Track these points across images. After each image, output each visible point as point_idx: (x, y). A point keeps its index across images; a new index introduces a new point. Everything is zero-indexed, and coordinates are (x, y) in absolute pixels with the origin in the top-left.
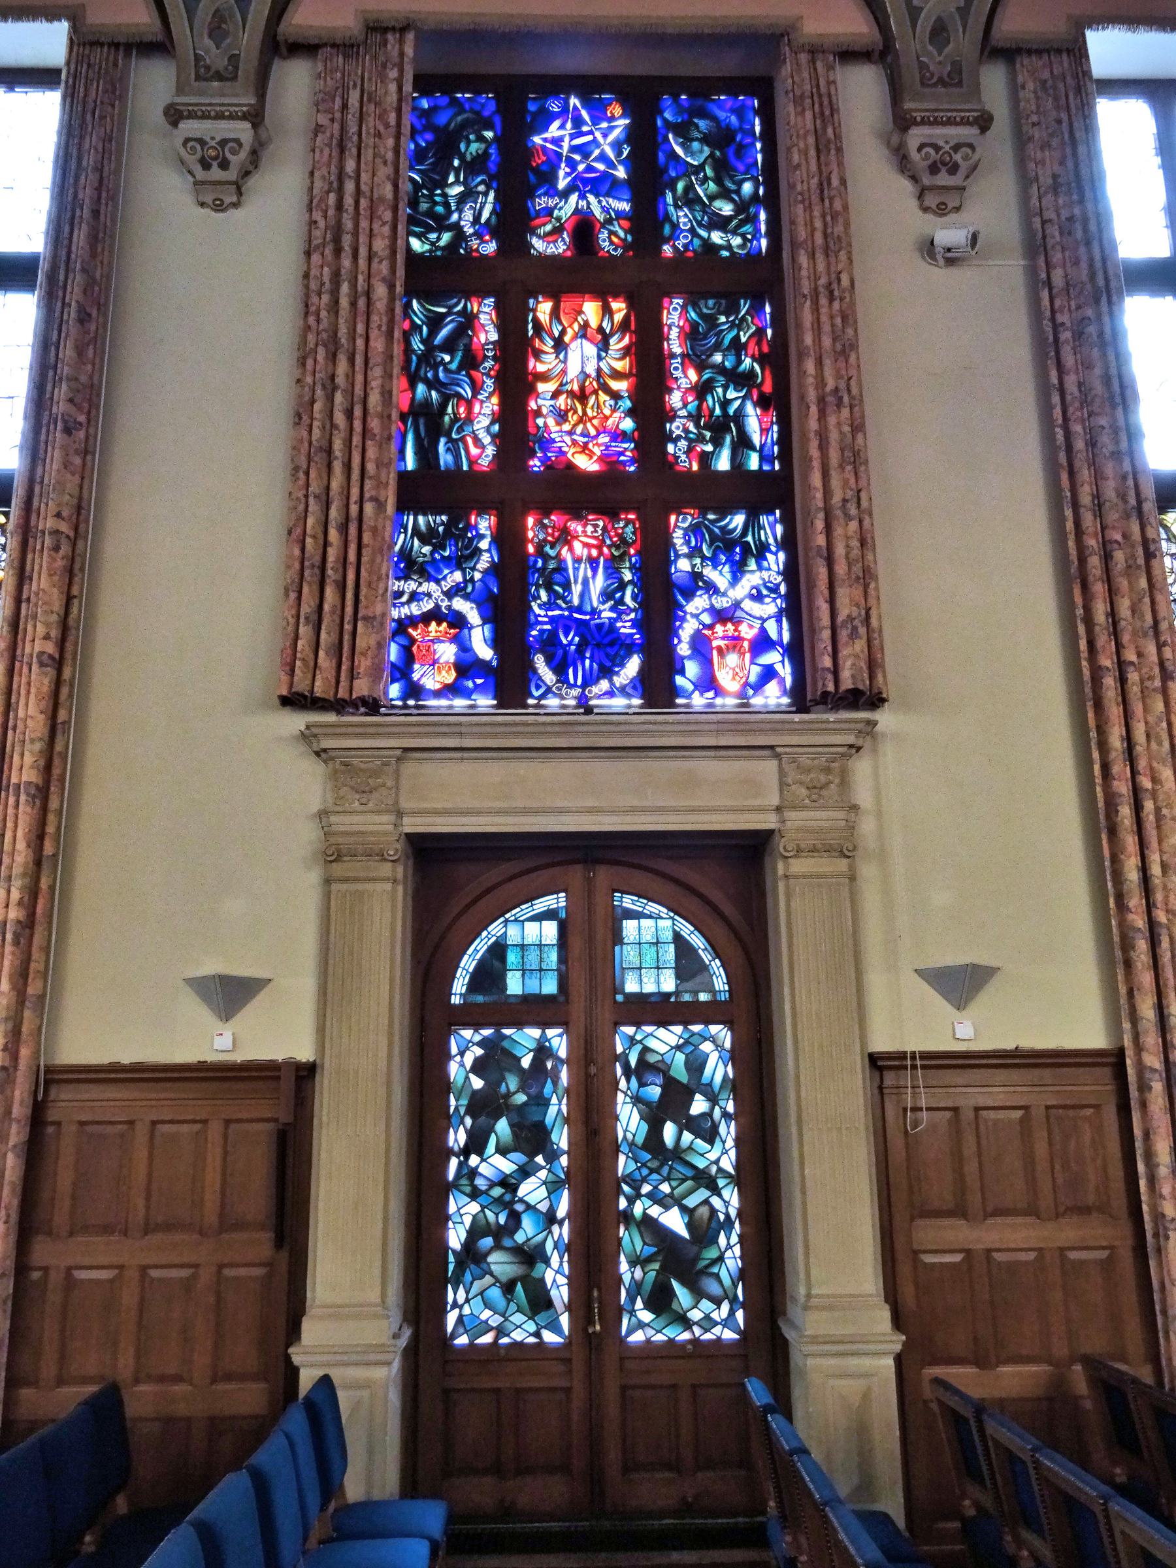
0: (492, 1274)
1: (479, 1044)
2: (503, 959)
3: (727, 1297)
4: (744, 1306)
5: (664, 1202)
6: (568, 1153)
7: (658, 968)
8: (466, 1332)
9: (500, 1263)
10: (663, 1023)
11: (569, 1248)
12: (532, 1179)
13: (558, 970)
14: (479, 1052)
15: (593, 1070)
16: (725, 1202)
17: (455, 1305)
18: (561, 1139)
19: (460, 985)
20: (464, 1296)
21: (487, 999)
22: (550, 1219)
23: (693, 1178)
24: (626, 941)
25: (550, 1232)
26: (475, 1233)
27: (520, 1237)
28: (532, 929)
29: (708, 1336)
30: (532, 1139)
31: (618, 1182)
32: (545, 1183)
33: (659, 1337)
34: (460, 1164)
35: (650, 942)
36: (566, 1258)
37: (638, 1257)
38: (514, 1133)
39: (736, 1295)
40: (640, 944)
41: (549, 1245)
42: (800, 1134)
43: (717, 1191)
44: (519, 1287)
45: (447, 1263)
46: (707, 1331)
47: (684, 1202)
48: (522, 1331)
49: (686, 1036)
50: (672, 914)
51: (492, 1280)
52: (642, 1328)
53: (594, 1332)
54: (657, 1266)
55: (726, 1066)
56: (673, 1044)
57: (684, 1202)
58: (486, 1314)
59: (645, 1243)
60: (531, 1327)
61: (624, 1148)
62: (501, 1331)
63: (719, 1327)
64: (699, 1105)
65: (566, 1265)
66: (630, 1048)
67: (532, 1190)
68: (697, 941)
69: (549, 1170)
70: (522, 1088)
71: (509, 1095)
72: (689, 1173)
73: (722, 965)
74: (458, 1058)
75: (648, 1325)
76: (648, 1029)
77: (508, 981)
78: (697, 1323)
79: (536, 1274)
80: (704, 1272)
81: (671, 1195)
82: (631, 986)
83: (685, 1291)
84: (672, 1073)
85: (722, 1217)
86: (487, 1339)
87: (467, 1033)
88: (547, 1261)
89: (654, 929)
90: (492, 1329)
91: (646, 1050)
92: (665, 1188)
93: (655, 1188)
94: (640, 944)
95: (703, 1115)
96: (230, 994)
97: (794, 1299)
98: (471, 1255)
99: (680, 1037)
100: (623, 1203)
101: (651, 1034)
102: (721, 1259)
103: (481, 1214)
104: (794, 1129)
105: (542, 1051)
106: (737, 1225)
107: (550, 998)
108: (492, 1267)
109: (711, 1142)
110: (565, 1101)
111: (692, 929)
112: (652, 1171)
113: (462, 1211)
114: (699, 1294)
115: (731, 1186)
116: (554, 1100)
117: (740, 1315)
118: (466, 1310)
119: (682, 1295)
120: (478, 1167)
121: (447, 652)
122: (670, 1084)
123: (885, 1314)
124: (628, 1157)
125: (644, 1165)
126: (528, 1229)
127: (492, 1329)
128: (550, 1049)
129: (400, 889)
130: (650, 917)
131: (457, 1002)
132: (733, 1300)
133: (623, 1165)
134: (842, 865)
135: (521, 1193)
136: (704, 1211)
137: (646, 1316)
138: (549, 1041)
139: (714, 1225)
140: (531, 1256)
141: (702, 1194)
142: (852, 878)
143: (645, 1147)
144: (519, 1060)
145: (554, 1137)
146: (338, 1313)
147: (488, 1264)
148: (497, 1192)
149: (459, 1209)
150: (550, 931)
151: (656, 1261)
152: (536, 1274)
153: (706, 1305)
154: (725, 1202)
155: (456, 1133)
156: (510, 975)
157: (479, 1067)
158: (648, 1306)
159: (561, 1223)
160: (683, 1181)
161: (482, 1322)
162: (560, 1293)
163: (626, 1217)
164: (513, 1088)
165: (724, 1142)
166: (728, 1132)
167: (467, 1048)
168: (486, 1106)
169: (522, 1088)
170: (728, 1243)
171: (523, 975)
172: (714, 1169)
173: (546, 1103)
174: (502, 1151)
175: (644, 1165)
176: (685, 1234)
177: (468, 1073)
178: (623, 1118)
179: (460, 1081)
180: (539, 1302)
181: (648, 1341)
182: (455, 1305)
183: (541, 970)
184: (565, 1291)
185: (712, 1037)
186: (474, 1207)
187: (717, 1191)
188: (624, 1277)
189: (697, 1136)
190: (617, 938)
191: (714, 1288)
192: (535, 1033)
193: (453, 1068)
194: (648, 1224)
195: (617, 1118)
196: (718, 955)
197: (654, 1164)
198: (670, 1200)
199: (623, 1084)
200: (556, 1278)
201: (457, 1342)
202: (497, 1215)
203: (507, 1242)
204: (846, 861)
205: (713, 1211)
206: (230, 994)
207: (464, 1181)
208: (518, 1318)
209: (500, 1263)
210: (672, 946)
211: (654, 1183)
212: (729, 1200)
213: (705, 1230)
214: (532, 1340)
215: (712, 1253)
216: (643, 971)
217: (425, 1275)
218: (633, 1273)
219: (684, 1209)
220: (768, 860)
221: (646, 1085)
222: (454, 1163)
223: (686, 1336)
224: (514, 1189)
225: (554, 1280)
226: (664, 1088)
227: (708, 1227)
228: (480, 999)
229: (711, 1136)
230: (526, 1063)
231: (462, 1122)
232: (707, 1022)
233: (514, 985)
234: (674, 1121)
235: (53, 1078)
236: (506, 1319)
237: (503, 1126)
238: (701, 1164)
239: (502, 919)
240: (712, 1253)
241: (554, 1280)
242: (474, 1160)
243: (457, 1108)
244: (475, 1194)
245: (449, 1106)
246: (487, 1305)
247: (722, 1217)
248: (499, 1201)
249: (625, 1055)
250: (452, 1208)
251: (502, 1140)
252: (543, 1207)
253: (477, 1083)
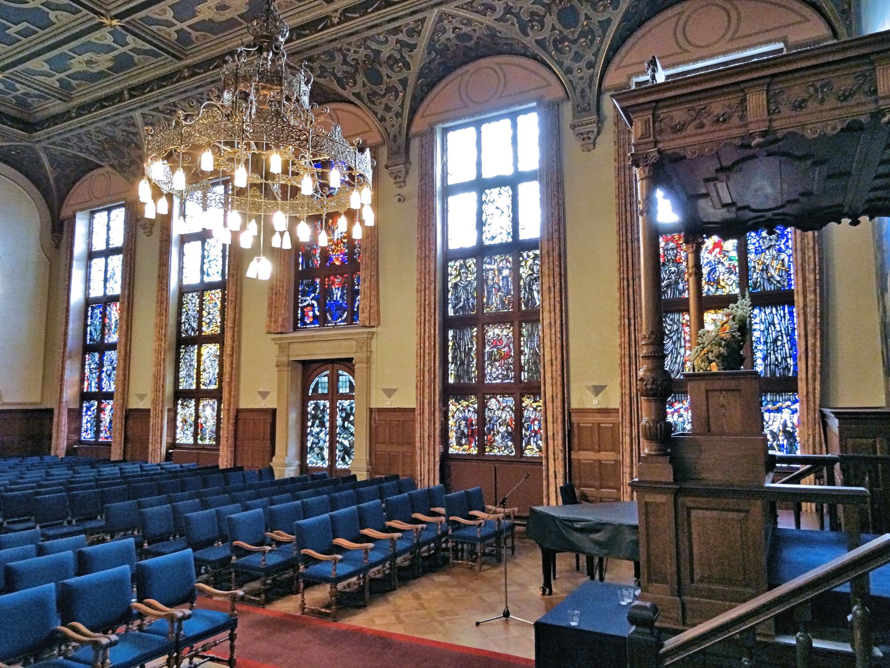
9: (317, 450)
18: (327, 424)
19: (311, 391)
22: (325, 442)
26: (313, 443)
30: (322, 424)
52: (340, 465)
82: (341, 391)
96: (264, 395)
98: (312, 448)
105: (324, 406)
114: (350, 459)
121: (311, 314)
122: (347, 413)
133: (338, 431)
140: (322, 449)
150: (326, 379)
162: (327, 457)
163: (338, 442)
168: (315, 417)
180: (323, 459)
190: (338, 381)
193: (309, 409)
194: (341, 443)
200: (326, 453)
206: (264, 395)
209: (317, 450)
217: (303, 452)
233: (320, 391)
235: (238, 411)
237: (317, 421)
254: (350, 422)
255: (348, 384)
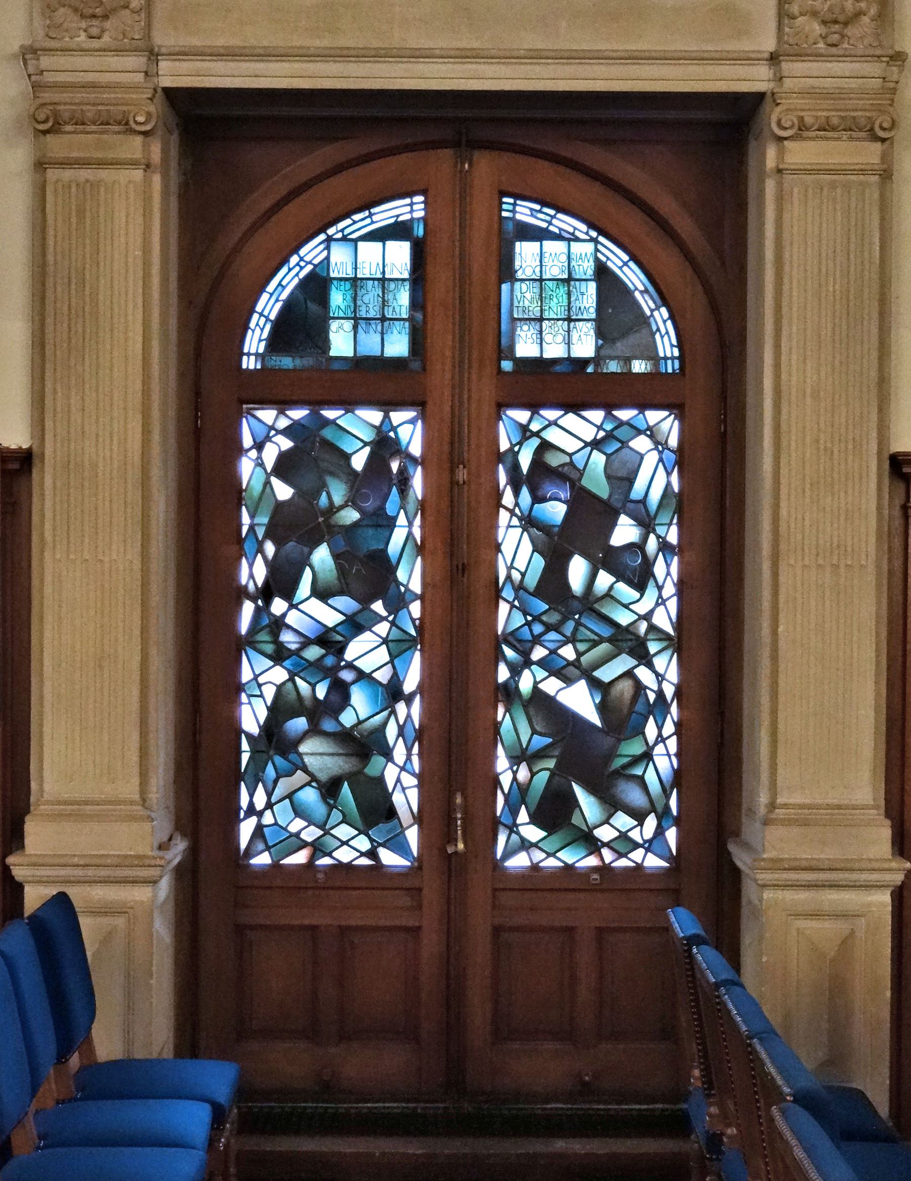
0: (305, 770)
1: (286, 432)
2: (324, 301)
3: (653, 809)
4: (677, 822)
5: (564, 673)
6: (422, 597)
7: (569, 320)
8: (268, 848)
9: (318, 755)
10: (574, 406)
11: (420, 735)
12: (367, 636)
13: (411, 319)
14: (286, 444)
15: (462, 474)
16: (657, 675)
17: (251, 811)
19: (255, 340)
20: (265, 799)
21: (298, 362)
22: (393, 693)
23: (610, 640)
24: (519, 275)
25: (393, 712)
26: (281, 710)
27: (347, 719)
28: (370, 252)
29: (623, 863)
30: (367, 576)
31: (496, 643)
32: (385, 641)
33: (552, 862)
34: (258, 610)
35: (558, 276)
36: (416, 749)
37: (524, 751)
38: (339, 567)
39: (667, 808)
40: (541, 280)
41: (391, 731)
42: (775, 574)
43: (645, 659)
44: (346, 789)
45: (239, 752)
46: (621, 855)
47: (597, 674)
48: (351, 847)
49: (609, 427)
50: (594, 234)
51: (307, 778)
52: (526, 849)
53: (456, 853)
54: (551, 764)
55: (669, 474)
56: (589, 439)
57: (597, 674)
58: (297, 825)
59: (534, 732)
60: (363, 843)
61: (508, 593)
62: (318, 848)
63: (641, 851)
64: (625, 532)
65: (415, 759)
66: (520, 443)
67: (367, 652)
68: (633, 277)
69: (393, 623)
70: (352, 501)
71: (332, 510)
72: (606, 631)
73: (672, 317)
74: (253, 454)
75: (535, 845)
76: (551, 414)
77: (332, 336)
78: (607, 845)
79: (371, 770)
80: (622, 773)
81: (576, 664)
82: (526, 347)
83: (592, 799)
84: (585, 482)
85: (652, 697)
86: (300, 858)
87: (267, 415)
88: (387, 754)
89: (564, 258)
90: (304, 845)
91: (546, 446)
92: (568, 652)
93: (553, 652)
94: (541, 280)
95: (630, 546)
97: (751, 812)
98: (273, 739)
99: (600, 428)
100: (503, 674)
101: (555, 423)
102: (647, 756)
103: (290, 685)
104: (766, 566)
105: (384, 445)
106: (674, 709)
107: (397, 363)
108: (307, 759)
109: (641, 587)
110: (418, 521)
111: (626, 258)
112: (549, 628)
113: (261, 680)
114: (612, 804)
115: (669, 652)
116: (402, 520)
117: (671, 835)
118: (268, 819)
119: (588, 805)
120: (284, 615)
122: (581, 500)
123: (885, 833)
124: (513, 606)
125: (537, 619)
126: (360, 706)
127: (304, 845)
128: (397, 441)
129: (157, 179)
130: (558, 237)
131: (252, 367)
132: (663, 815)
133: (506, 617)
134: (871, 153)
135: (349, 655)
136: (626, 687)
137: (533, 833)
138: (394, 429)
139: (640, 707)
140: (365, 745)
141: (624, 663)
142: (886, 175)
143: (540, 592)
144: (347, 457)
145: (401, 575)
146: (75, 811)
147: (300, 755)
148: (313, 653)
149: (256, 677)
150: (399, 255)
151: (552, 757)
152: (371, 770)
153: (622, 821)
154: (657, 675)
155: (251, 566)
156: (334, 325)
157: (285, 467)
158: (536, 819)
159: (409, 700)
160: (595, 644)
161: (291, 835)
162: (406, 798)
163: (509, 693)
164: (338, 500)
165: (660, 588)
166: (667, 572)
167: (268, 438)
168: (297, 527)
169: (352, 501)
170: (660, 735)
171: (355, 328)
172: (643, 627)
173: (391, 523)
174: (321, 593)
175: (537, 619)
176: (595, 719)
177: (268, 476)
178: (507, 549)
179: (257, 486)
180: (376, 811)
181: (535, 867)
182: (251, 811)
183: (383, 319)
184: (413, 796)
185: (649, 428)
186: (279, 675)
187: (645, 659)
188: (501, 777)
189: (620, 575)
190: (506, 271)
191: (635, 797)
192: (374, 416)
193: (246, 466)
195: (498, 548)
196: (664, 300)
197: (553, 618)
198: (572, 671)
199: (508, 499)
201: (255, 861)
202: (313, 686)
203: (328, 725)
204: (878, 146)
205: (639, 688)
207: (264, 636)
208: (344, 831)
209: (318, 755)
210: (592, 287)
211: (552, 646)
212: (664, 672)
213: (624, 713)
214: (365, 861)
215: (635, 748)
216: (545, 324)
217: (205, 769)
218: (515, 773)
219: (595, 684)
220: (753, 144)
221: (544, 500)
222: (248, 609)
223: (592, 861)
224: (340, 650)
225: (398, 780)
226: (572, 505)
227: (631, 711)
228: (287, 362)
229: (641, 579)
230: (359, 462)
231: (260, 550)
232: (643, 407)
233: (341, 342)
234: (585, 555)
236: (327, 833)
237: (322, 556)
238: (624, 618)
239: (322, 237)
240: (635, 748)
241: (398, 780)
242: (278, 606)
243: (252, 528)
244: (279, 655)
245: (240, 525)
246: (298, 812)
247: (652, 697)
248: (317, 665)
249: (513, 454)
250: (246, 675)
251: (321, 576)
252: (383, 676)
253: (283, 491)
254: (607, 559)
255: (588, 297)
